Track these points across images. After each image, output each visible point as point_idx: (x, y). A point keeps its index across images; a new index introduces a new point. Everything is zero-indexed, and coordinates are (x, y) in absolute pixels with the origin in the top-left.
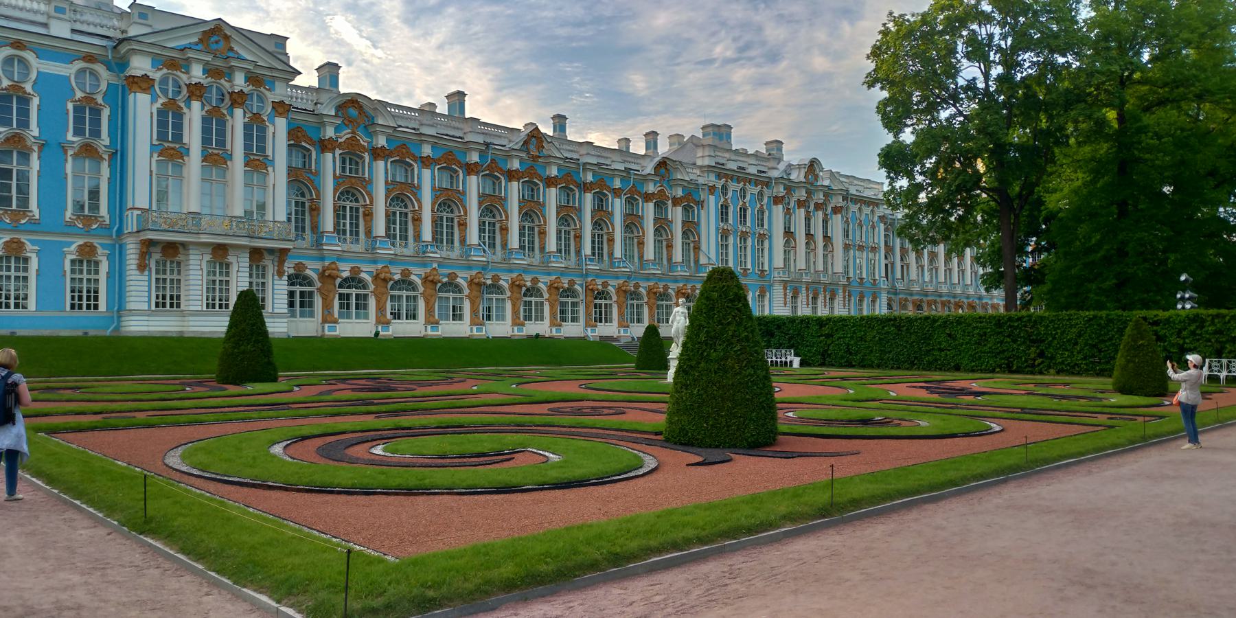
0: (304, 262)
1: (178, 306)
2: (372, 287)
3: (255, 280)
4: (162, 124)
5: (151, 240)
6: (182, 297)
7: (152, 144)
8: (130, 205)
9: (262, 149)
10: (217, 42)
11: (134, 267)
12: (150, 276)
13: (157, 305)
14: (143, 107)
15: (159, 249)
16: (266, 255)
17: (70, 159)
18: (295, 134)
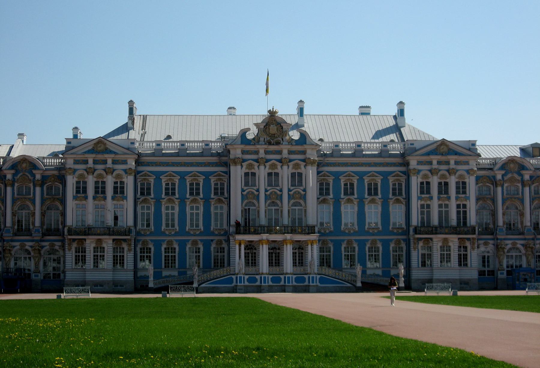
2: (523, 251)
4: (422, 188)
9: (464, 193)
13: (422, 266)
14: (415, 182)
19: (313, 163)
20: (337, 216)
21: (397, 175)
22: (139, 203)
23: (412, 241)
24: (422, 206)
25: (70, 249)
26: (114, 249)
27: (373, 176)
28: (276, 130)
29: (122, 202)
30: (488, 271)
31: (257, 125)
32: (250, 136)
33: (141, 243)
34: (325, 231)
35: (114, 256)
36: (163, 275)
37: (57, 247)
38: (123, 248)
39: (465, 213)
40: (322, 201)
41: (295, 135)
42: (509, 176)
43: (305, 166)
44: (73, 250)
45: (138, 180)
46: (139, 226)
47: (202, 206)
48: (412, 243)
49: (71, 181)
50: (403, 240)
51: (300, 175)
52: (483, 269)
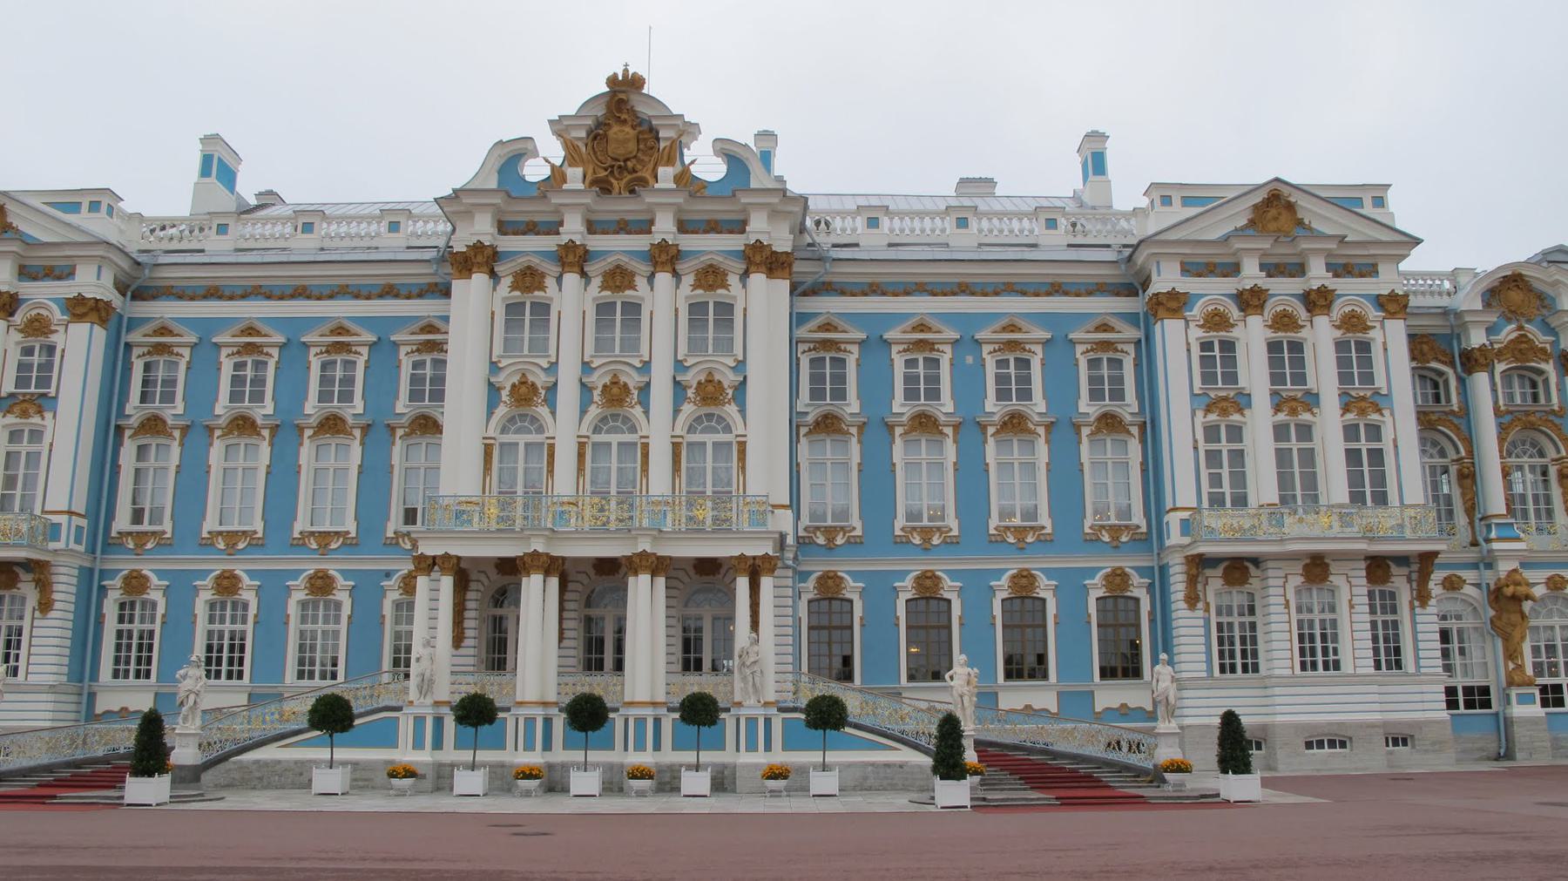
0: (1459, 573)
1: (1256, 669)
3: (1380, 618)
4: (1207, 362)
5: (1200, 556)
6: (1261, 654)
7: (1193, 395)
8: (1169, 505)
10: (1276, 219)
11: (1183, 605)
12: (1207, 621)
13: (1222, 670)
14: (1177, 342)
15: (1219, 571)
16: (1394, 569)
18: (1420, 345)
19: (770, 262)
20: (877, 484)
21: (1104, 327)
22: (128, 433)
24: (1211, 433)
27: (1012, 328)
28: (632, 146)
29: (36, 420)
31: (560, 127)
32: (535, 171)
33: (117, 582)
34: (831, 540)
38: (23, 600)
39: (1377, 456)
40: (817, 423)
41: (708, 167)
42: (1508, 333)
43: (745, 274)
45: (136, 352)
46: (122, 522)
51: (725, 309)
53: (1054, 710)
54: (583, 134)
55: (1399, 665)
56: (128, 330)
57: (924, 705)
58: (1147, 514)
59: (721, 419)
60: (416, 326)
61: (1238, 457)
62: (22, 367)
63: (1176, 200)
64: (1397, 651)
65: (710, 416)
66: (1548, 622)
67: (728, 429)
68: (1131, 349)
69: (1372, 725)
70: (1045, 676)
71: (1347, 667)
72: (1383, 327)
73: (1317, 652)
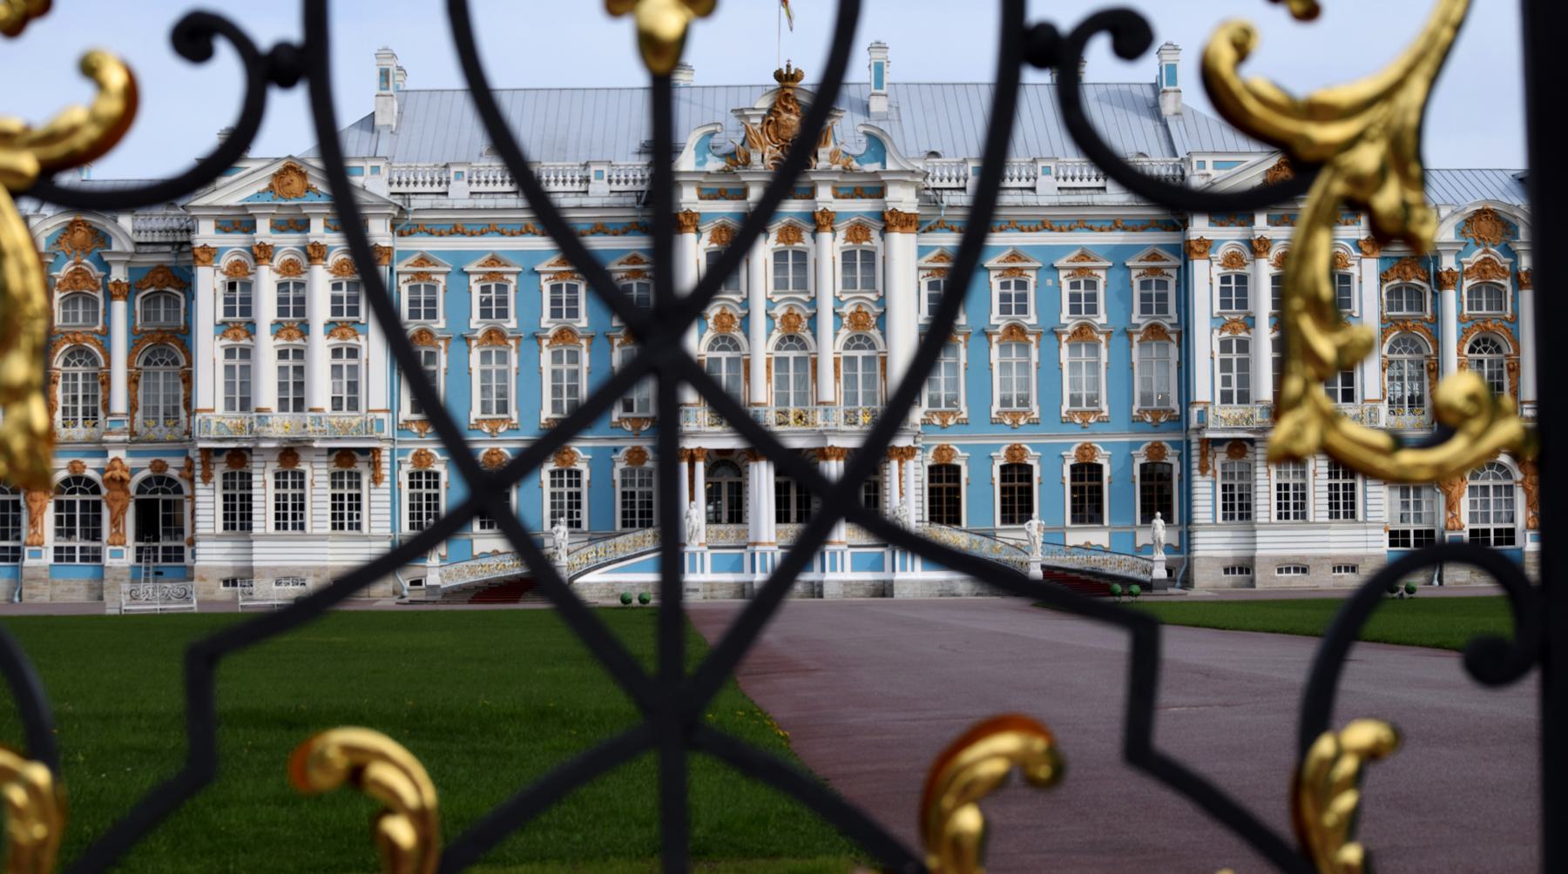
4: (1225, 292)
12: (1214, 483)
13: (1225, 517)
15: (1225, 448)
17: (1136, 345)
23: (1194, 446)
24: (1225, 346)
25: (207, 478)
26: (333, 475)
30: (1417, 533)
33: (409, 459)
35: (334, 497)
36: (476, 552)
37: (173, 473)
38: (358, 475)
42: (1476, 256)
44: (218, 479)
47: (584, 349)
48: (1195, 452)
49: (209, 283)
50: (1175, 445)
51: (869, 256)
52: (1403, 527)
53: (1106, 545)
54: (759, 121)
55: (1353, 515)
56: (399, 261)
57: (1012, 542)
58: (1180, 402)
59: (868, 339)
60: (624, 258)
61: (1244, 365)
62: (335, 299)
63: (1209, 165)
64: (1353, 506)
65: (859, 337)
66: (1485, 483)
67: (872, 347)
68: (1174, 273)
69: (1323, 558)
70: (1101, 521)
71: (1311, 518)
72: (1360, 265)
73: (1292, 505)
